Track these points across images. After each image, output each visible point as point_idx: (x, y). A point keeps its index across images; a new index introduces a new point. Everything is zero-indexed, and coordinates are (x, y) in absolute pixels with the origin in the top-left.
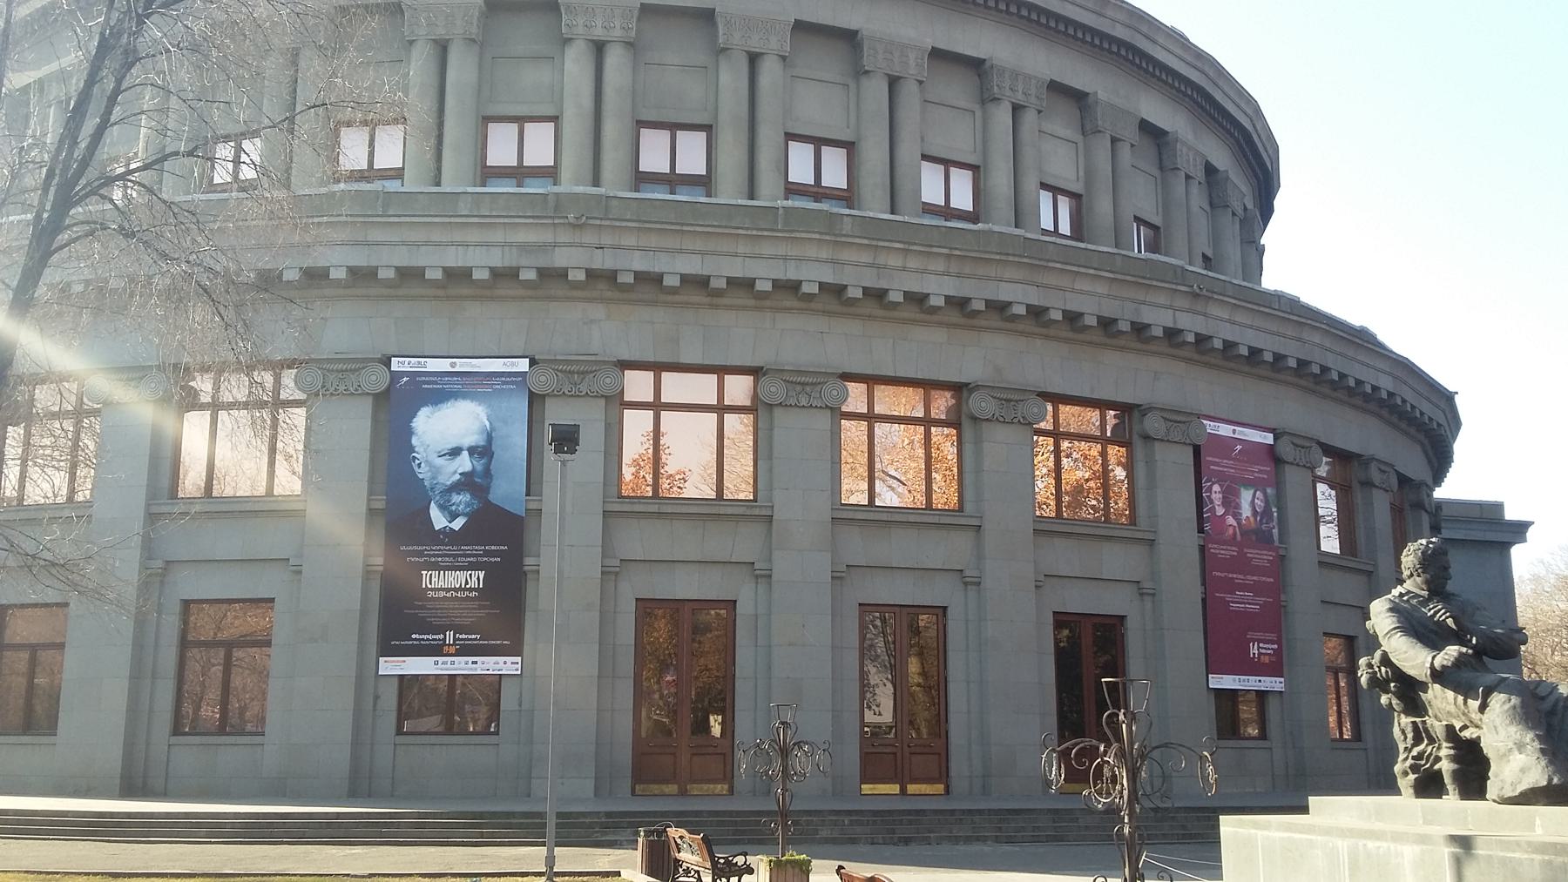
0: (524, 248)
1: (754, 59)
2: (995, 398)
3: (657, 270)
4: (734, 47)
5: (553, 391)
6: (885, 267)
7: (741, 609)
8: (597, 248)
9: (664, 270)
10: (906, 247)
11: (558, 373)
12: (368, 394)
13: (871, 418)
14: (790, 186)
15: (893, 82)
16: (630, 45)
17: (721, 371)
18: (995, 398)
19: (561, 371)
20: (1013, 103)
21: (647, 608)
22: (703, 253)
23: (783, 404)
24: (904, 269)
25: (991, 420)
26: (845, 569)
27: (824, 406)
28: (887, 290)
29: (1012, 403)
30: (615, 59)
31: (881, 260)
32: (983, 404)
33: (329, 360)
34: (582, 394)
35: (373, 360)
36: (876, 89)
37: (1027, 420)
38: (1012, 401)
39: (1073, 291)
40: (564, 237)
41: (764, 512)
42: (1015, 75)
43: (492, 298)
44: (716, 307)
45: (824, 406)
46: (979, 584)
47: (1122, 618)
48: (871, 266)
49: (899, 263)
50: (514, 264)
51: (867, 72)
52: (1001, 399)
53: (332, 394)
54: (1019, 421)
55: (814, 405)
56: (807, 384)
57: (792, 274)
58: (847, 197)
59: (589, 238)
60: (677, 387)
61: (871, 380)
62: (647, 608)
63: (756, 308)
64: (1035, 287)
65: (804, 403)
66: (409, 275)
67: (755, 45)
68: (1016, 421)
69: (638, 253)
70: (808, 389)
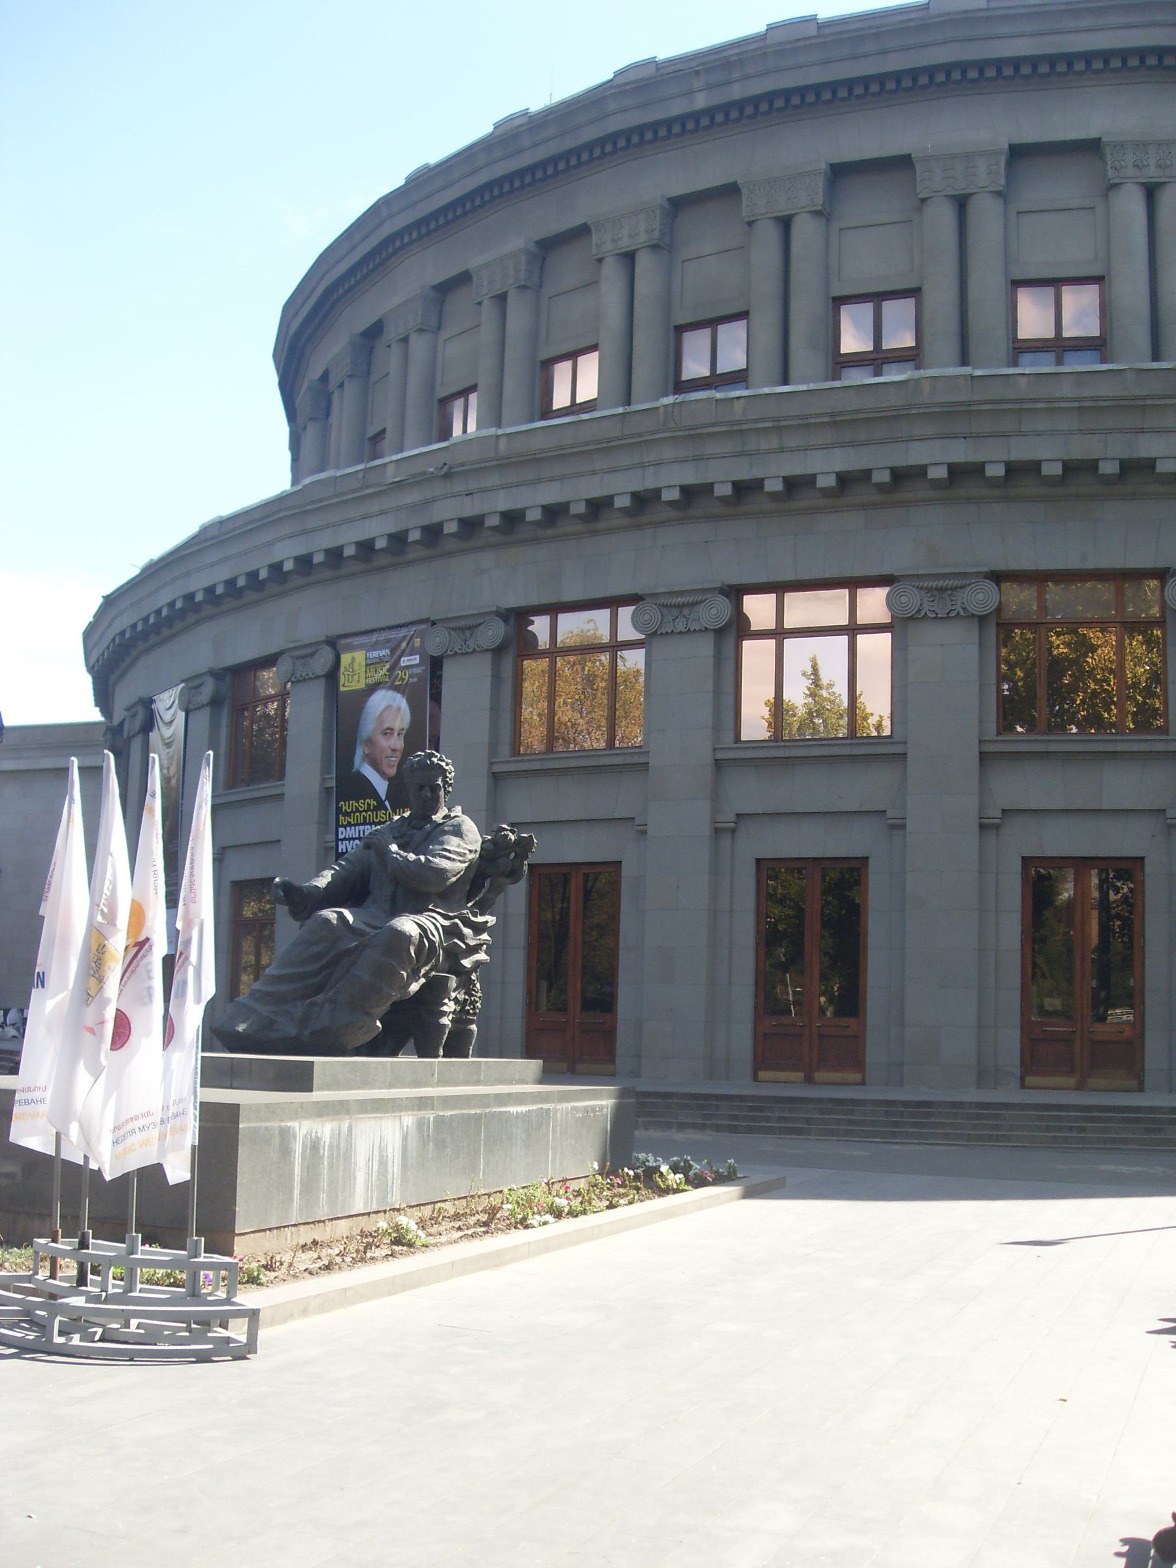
0: (413, 508)
1: (786, 224)
2: (922, 588)
3: (519, 506)
4: (759, 217)
5: (446, 651)
6: (757, 453)
7: (627, 871)
8: (467, 495)
9: (525, 505)
10: (776, 424)
11: (453, 633)
12: (320, 676)
13: (780, 634)
14: (842, 359)
15: (961, 203)
16: (655, 247)
17: (612, 603)
18: (922, 588)
19: (453, 629)
20: (1142, 184)
21: (766, 868)
22: (561, 478)
23: (659, 633)
24: (782, 450)
25: (917, 618)
26: (733, 818)
27: (703, 629)
28: (763, 479)
29: (950, 592)
30: (644, 262)
31: (751, 446)
32: (904, 599)
33: (295, 648)
34: (471, 650)
35: (318, 643)
36: (943, 217)
37: (969, 611)
38: (946, 589)
39: (1020, 434)
40: (438, 489)
41: (642, 760)
42: (1142, 145)
43: (409, 563)
44: (595, 533)
45: (703, 629)
46: (904, 826)
47: (1143, 858)
48: (743, 454)
49: (775, 444)
50: (404, 529)
51: (923, 200)
52: (929, 589)
53: (299, 681)
54: (958, 612)
55: (692, 629)
56: (684, 605)
57: (651, 484)
58: (911, 357)
59: (459, 486)
60: (572, 626)
61: (780, 588)
62: (766, 868)
63: (639, 527)
64: (962, 439)
65: (681, 628)
66: (335, 555)
67: (783, 209)
68: (952, 614)
69: (502, 493)
70: (686, 611)
